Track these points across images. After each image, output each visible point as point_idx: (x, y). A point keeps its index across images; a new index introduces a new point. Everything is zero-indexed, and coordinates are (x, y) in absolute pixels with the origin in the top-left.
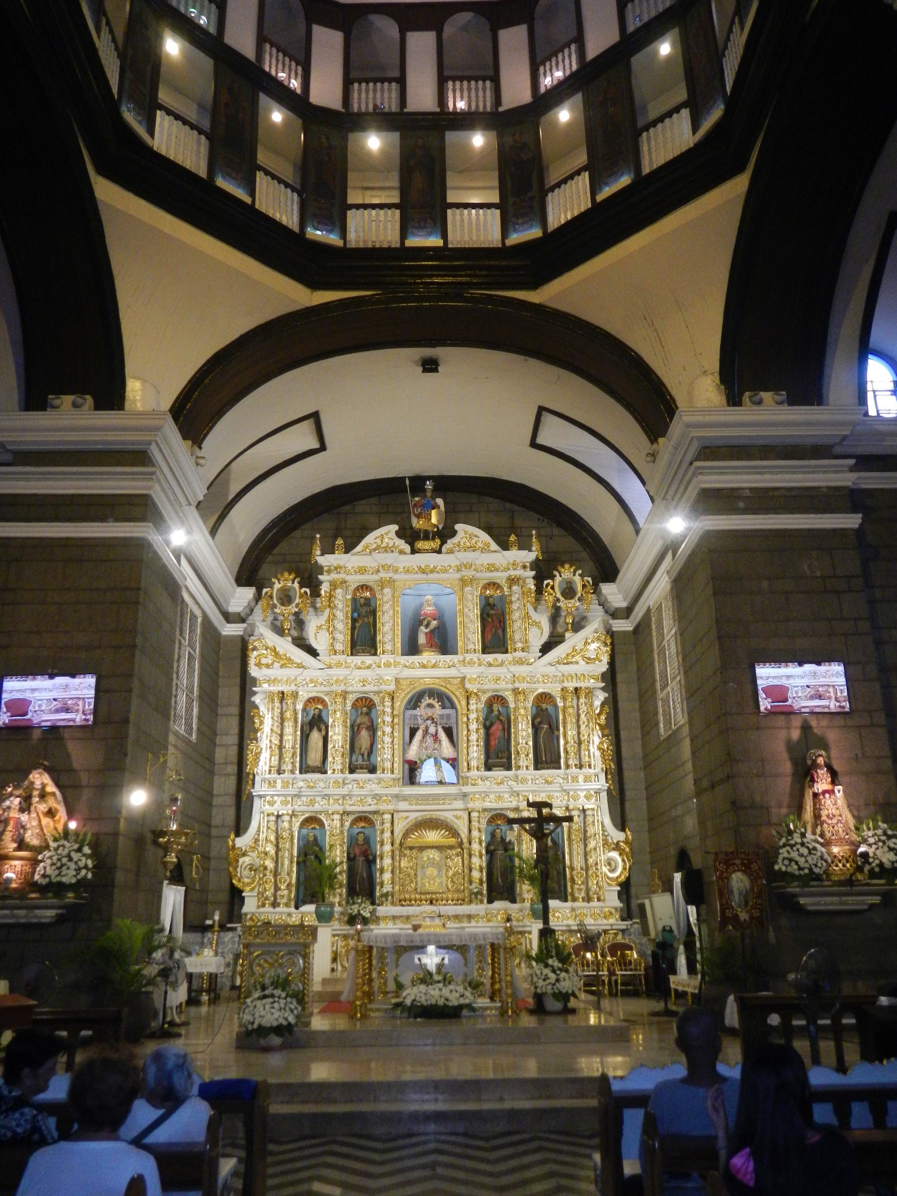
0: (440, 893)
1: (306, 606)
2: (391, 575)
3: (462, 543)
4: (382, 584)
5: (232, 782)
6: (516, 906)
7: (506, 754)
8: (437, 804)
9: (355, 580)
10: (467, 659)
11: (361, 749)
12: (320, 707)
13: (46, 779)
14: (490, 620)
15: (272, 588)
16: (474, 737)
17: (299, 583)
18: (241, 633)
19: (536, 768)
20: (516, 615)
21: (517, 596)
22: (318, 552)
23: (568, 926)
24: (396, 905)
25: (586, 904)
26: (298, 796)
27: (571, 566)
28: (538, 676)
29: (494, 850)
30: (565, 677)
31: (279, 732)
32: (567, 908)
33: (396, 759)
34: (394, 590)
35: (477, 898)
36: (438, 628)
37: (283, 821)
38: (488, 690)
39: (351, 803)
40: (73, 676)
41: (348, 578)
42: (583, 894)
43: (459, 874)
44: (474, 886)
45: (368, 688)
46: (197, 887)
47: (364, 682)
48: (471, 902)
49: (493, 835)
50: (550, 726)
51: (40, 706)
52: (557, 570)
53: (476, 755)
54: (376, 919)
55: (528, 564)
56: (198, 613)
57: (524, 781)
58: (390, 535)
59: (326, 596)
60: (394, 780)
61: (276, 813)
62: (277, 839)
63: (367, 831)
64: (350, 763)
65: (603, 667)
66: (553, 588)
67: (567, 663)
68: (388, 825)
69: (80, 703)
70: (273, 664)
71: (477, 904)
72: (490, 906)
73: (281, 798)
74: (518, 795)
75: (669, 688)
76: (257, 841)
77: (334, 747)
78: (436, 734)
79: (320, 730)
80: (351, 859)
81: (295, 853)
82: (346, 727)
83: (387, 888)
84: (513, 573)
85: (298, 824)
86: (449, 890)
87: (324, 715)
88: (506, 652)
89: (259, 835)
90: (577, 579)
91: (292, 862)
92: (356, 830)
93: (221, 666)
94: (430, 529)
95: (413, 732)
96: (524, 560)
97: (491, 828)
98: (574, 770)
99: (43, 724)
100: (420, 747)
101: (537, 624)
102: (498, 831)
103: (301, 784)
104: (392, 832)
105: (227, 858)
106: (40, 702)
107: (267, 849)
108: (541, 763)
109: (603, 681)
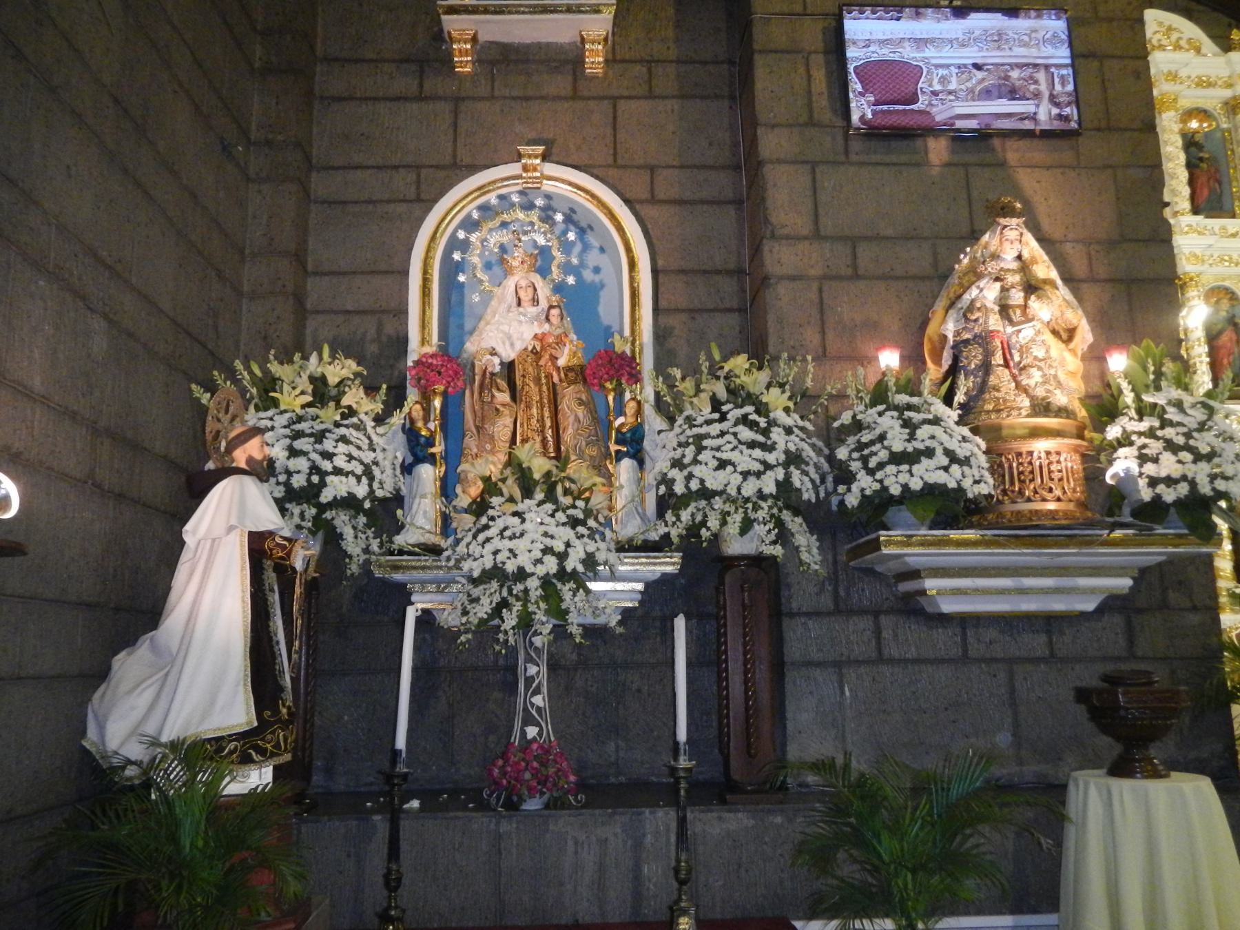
13: (1032, 248)
40: (1012, 12)
51: (943, 80)
69: (1041, 76)
99: (960, 124)
106: (942, 72)
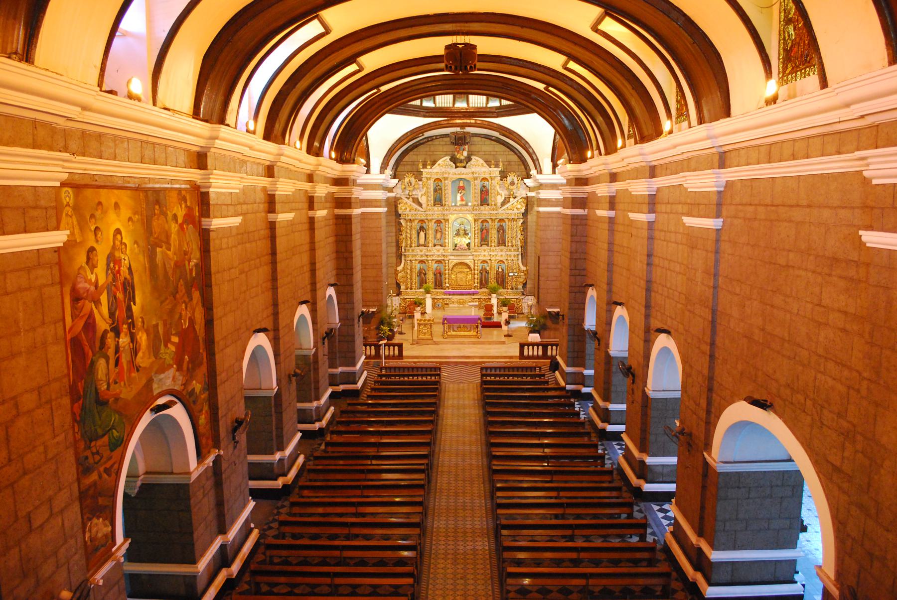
65: (523, 211)
98: (510, 248)
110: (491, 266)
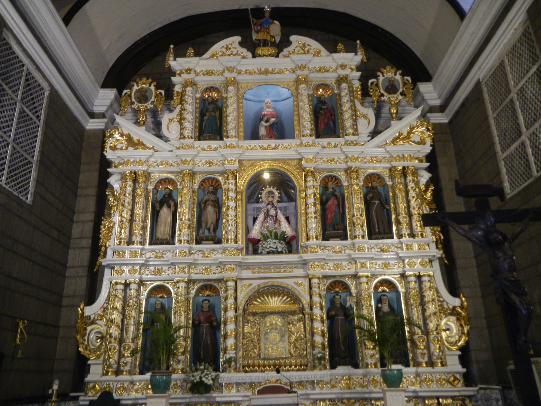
0: (283, 359)
1: (160, 104)
2: (234, 74)
3: (296, 51)
4: (228, 83)
5: (86, 255)
6: (360, 371)
7: (341, 226)
8: (278, 272)
9: (203, 81)
10: (304, 142)
11: (207, 224)
12: (170, 187)
14: (322, 112)
15: (131, 89)
16: (312, 209)
17: (155, 86)
18: (103, 127)
19: (370, 238)
20: (346, 107)
21: (346, 91)
22: (171, 58)
23: (415, 392)
24: (239, 372)
25: (430, 369)
26: (145, 265)
27: (392, 68)
28: (368, 158)
29: (335, 315)
30: (392, 158)
31: (130, 207)
32: (410, 373)
33: (240, 231)
34: (238, 90)
35: (320, 364)
36: (276, 124)
37: (130, 289)
38: (323, 170)
39: (196, 272)
41: (197, 79)
42: (426, 359)
43: (303, 339)
44: (316, 351)
45: (213, 168)
46: (19, 355)
47: (210, 163)
48: (314, 368)
49: (332, 302)
50: (380, 201)
52: (380, 71)
53: (314, 226)
54: (220, 388)
55: (354, 67)
56: (44, 85)
57: (361, 249)
58: (234, 45)
59: (178, 95)
60: (237, 249)
61: (123, 282)
62: (124, 307)
63: (212, 300)
64: (197, 235)
65: (427, 149)
66: (377, 85)
67: (394, 145)
68: (231, 292)
70: (127, 148)
71: (320, 370)
72: (333, 371)
73: (129, 267)
74: (356, 263)
75: (523, 137)
76: (105, 309)
77: (181, 220)
78: (276, 216)
79: (169, 206)
80: (196, 326)
81: (142, 320)
82: (193, 203)
83: (231, 354)
84: (342, 72)
85: (146, 293)
86: (292, 356)
87: (174, 195)
88: (339, 137)
89: (108, 304)
90: (398, 77)
91: (138, 329)
92: (201, 299)
93: (83, 154)
94: (268, 38)
95: (255, 219)
96: (351, 63)
97: (330, 296)
100: (262, 226)
101: (365, 116)
102: (338, 297)
103: (149, 255)
104: (236, 299)
105: (75, 327)
107: (113, 317)
108: (375, 234)
109: (427, 161)
110: (359, 295)
